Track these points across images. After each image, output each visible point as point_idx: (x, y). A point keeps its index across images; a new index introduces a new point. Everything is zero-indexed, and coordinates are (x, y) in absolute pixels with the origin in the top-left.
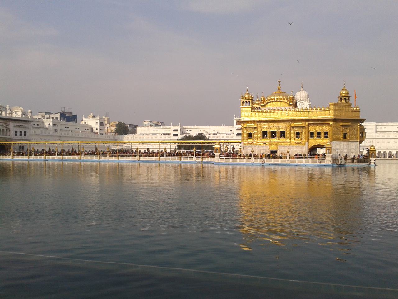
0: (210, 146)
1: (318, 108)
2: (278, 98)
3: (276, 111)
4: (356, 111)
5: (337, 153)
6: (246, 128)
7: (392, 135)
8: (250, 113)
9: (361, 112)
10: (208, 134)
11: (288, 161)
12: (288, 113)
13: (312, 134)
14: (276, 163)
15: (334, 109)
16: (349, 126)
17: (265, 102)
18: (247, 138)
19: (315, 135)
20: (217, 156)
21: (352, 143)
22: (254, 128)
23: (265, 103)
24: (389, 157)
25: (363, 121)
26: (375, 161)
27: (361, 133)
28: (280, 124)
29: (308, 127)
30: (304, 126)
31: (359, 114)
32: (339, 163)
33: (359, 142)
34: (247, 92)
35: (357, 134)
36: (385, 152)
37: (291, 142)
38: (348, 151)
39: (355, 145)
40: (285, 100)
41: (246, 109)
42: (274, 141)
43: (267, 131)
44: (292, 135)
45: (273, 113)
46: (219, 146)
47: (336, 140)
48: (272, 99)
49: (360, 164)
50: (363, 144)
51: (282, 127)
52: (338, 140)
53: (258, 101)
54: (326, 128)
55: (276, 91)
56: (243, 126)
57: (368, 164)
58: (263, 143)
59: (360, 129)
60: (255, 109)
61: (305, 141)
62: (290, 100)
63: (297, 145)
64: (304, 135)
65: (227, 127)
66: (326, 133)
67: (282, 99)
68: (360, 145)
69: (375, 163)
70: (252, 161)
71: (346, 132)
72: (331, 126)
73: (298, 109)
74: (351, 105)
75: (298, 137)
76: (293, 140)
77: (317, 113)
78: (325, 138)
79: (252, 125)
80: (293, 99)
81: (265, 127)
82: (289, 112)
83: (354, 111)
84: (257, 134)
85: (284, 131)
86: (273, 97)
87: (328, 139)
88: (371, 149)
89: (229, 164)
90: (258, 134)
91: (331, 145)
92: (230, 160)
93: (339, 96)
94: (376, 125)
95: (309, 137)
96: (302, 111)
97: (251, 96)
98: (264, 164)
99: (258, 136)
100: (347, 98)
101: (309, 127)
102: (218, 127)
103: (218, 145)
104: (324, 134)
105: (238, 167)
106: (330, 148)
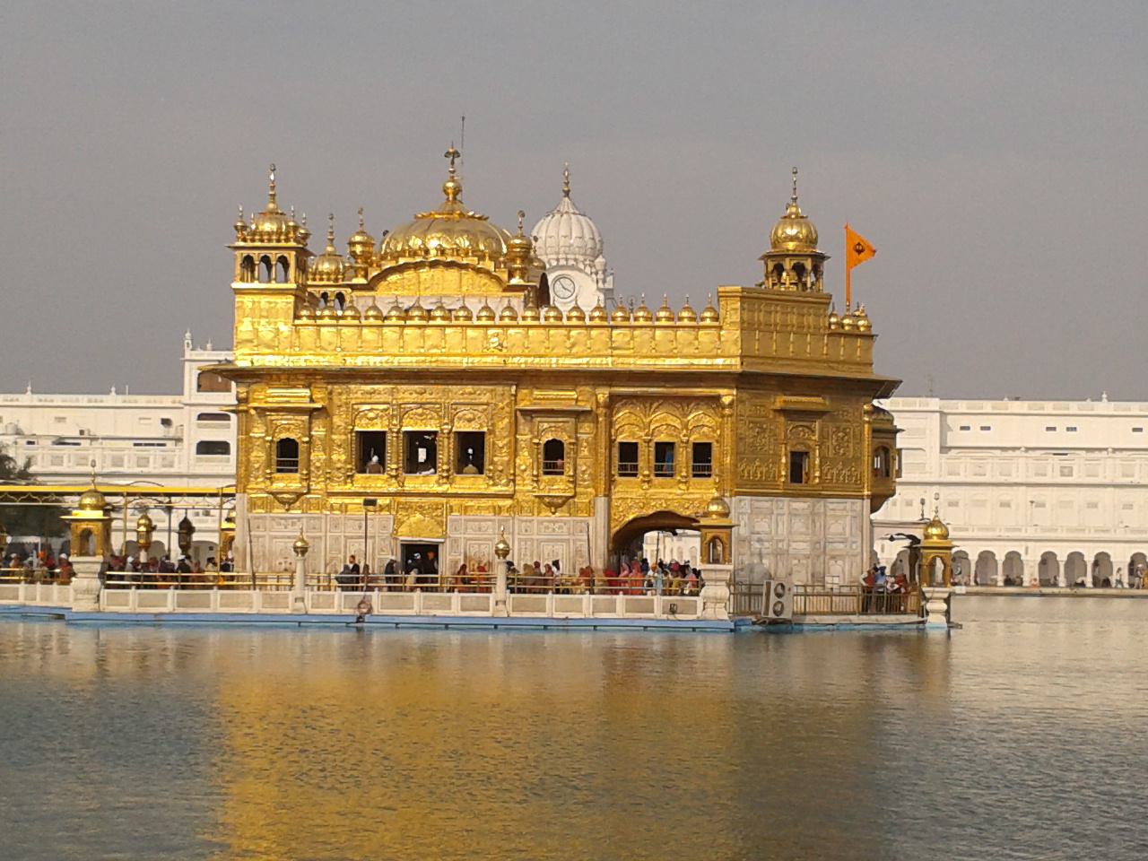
0: (45, 515)
1: (662, 314)
2: (445, 245)
3: (434, 318)
4: (854, 335)
5: (756, 560)
6: (262, 412)
7: (1109, 469)
8: (285, 329)
9: (877, 344)
10: (23, 442)
11: (499, 602)
12: (500, 331)
13: (629, 452)
14: (433, 612)
15: (742, 321)
17: (373, 268)
18: (269, 466)
19: (646, 457)
21: (833, 504)
22: (311, 413)
23: (374, 273)
24: (1008, 582)
25: (885, 388)
26: (947, 601)
27: (876, 453)
28: (458, 392)
29: (599, 420)
30: (588, 408)
31: (869, 348)
32: (771, 615)
33: (867, 503)
34: (271, 206)
35: (857, 459)
36: (986, 557)
37: (518, 496)
38: (814, 549)
39: (848, 518)
40: (481, 258)
41: (264, 300)
42: (425, 488)
43: (383, 434)
44: (524, 460)
45: (418, 331)
46: (99, 514)
47: (754, 484)
48: (414, 254)
49: (874, 617)
50: (887, 512)
51: (470, 411)
53: (333, 257)
54: (701, 424)
55: (434, 204)
57: (915, 618)
58: (360, 500)
59: (874, 431)
60: (313, 302)
62: (513, 260)
63: (546, 515)
64: (586, 459)
65: (142, 400)
66: (702, 453)
67: (467, 254)
68: (873, 516)
69: (947, 613)
70: (299, 605)
71: (801, 448)
72: (727, 411)
73: (552, 314)
74: (825, 301)
75: (555, 466)
76: (525, 487)
77: (653, 338)
78: (695, 476)
79: (299, 396)
80: (526, 253)
81: (373, 410)
82: (509, 326)
83: (846, 335)
84: (328, 446)
86: (415, 242)
87: (710, 480)
88: (927, 537)
89: (158, 621)
90: (330, 449)
91: (726, 515)
92: (169, 600)
93: (770, 250)
94: (943, 414)
95: (615, 471)
96: (574, 322)
97: (296, 228)
98: (367, 618)
99: (335, 457)
100: (808, 264)
101: (612, 416)
102: (83, 400)
103: (95, 507)
104: (691, 455)
105: (214, 637)
106: (722, 533)
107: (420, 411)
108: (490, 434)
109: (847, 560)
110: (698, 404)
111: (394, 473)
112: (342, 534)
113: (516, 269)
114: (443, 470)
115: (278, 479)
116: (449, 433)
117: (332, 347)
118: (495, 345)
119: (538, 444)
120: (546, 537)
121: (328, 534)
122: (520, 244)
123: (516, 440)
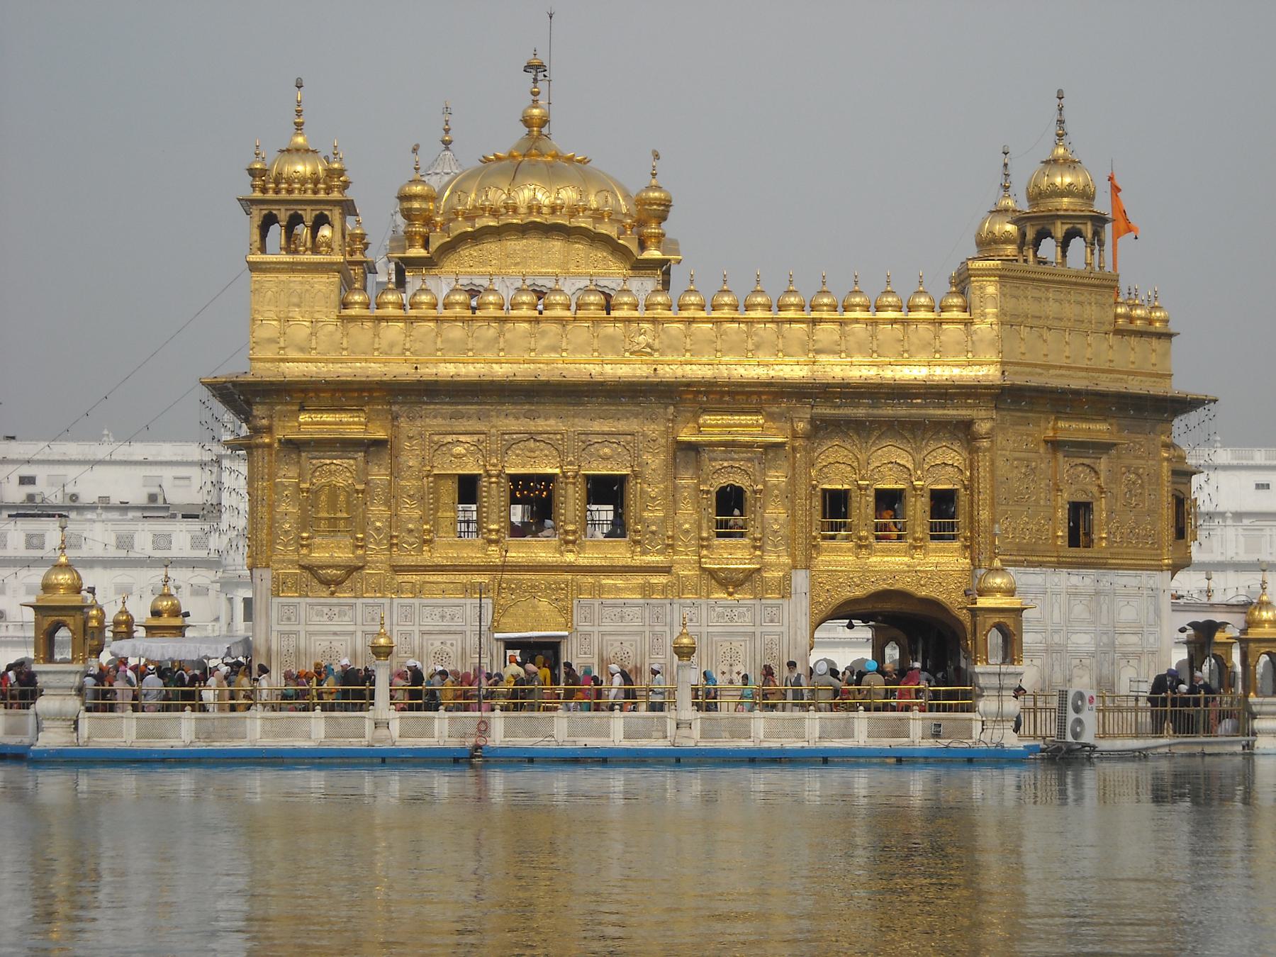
13: (836, 504)
16: (1103, 448)
17: (434, 238)
19: (863, 510)
20: (61, 691)
31: (1166, 354)
44: (687, 515)
48: (494, 213)
52: (1033, 552)
54: (942, 465)
56: (269, 430)
61: (786, 560)
71: (1081, 498)
78: (933, 538)
79: (351, 424)
85: (622, 480)
86: (497, 197)
99: (404, 512)
107: (532, 444)
108: (636, 477)
109: (1145, 659)
110: (938, 432)
111: (494, 537)
112: (416, 629)
113: (651, 236)
114: (567, 532)
115: (320, 547)
116: (574, 477)
117: (397, 350)
118: (636, 348)
119: (708, 492)
120: (720, 629)
121: (395, 629)
122: (660, 199)
123: (675, 487)
